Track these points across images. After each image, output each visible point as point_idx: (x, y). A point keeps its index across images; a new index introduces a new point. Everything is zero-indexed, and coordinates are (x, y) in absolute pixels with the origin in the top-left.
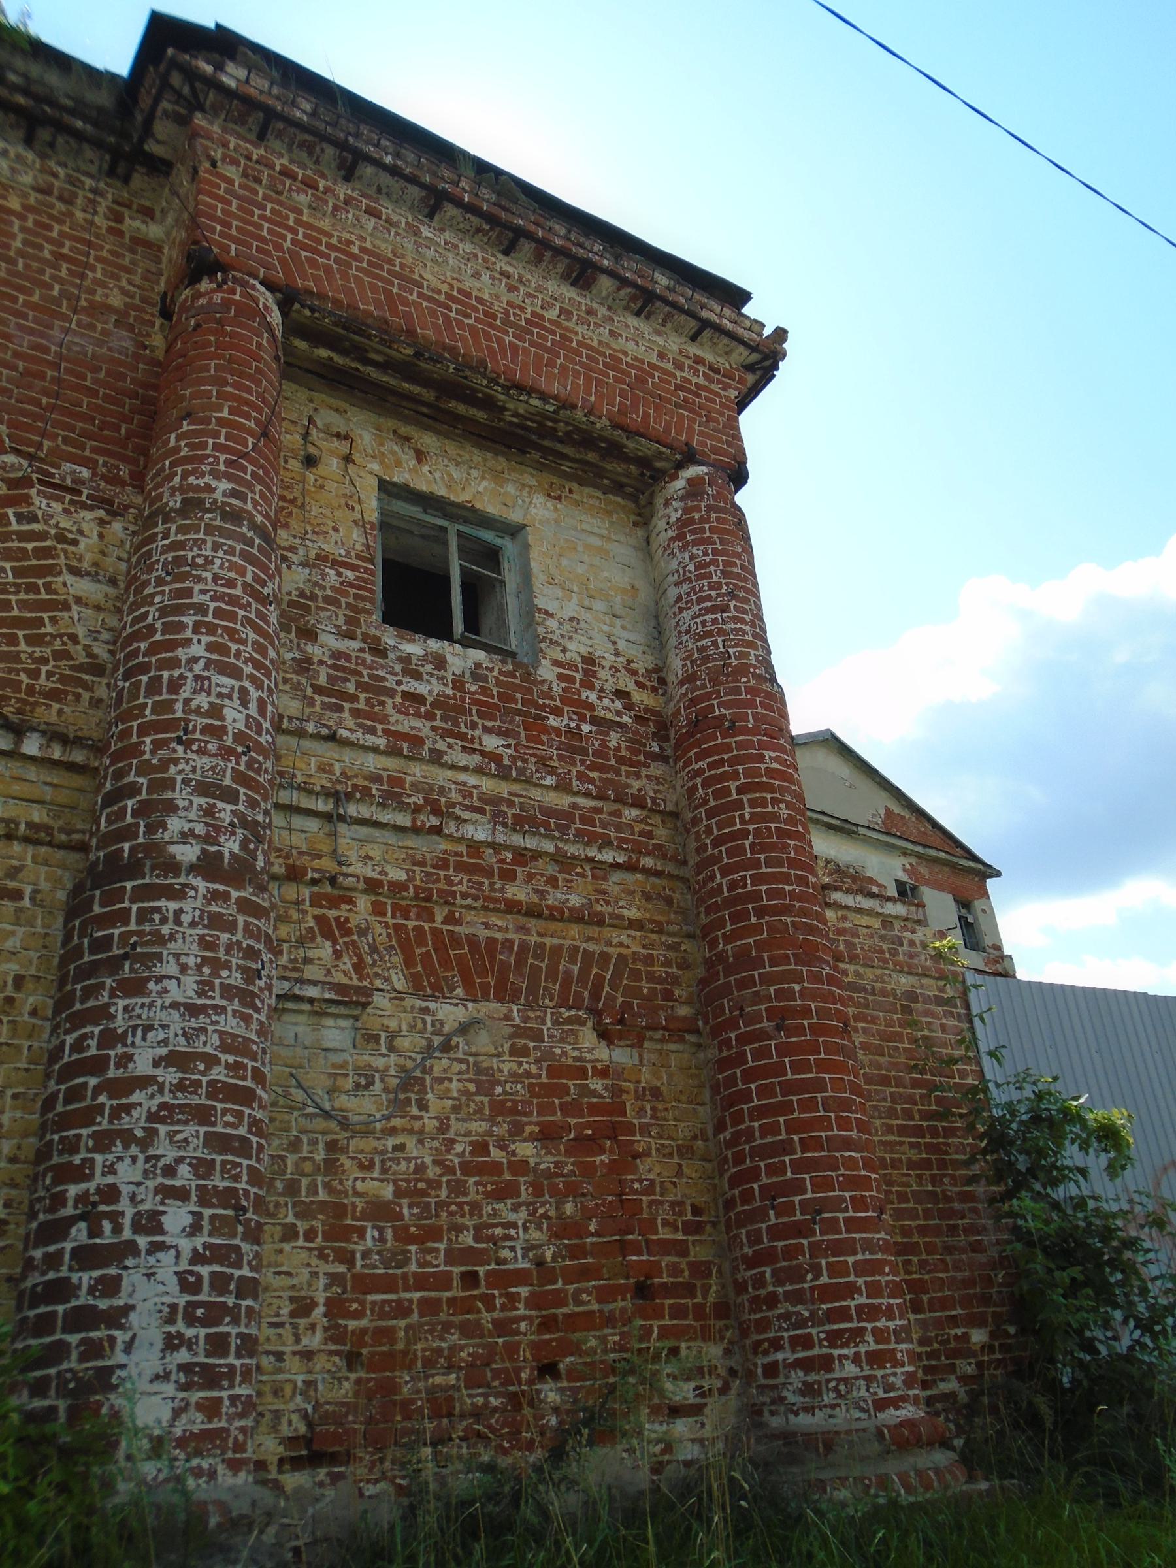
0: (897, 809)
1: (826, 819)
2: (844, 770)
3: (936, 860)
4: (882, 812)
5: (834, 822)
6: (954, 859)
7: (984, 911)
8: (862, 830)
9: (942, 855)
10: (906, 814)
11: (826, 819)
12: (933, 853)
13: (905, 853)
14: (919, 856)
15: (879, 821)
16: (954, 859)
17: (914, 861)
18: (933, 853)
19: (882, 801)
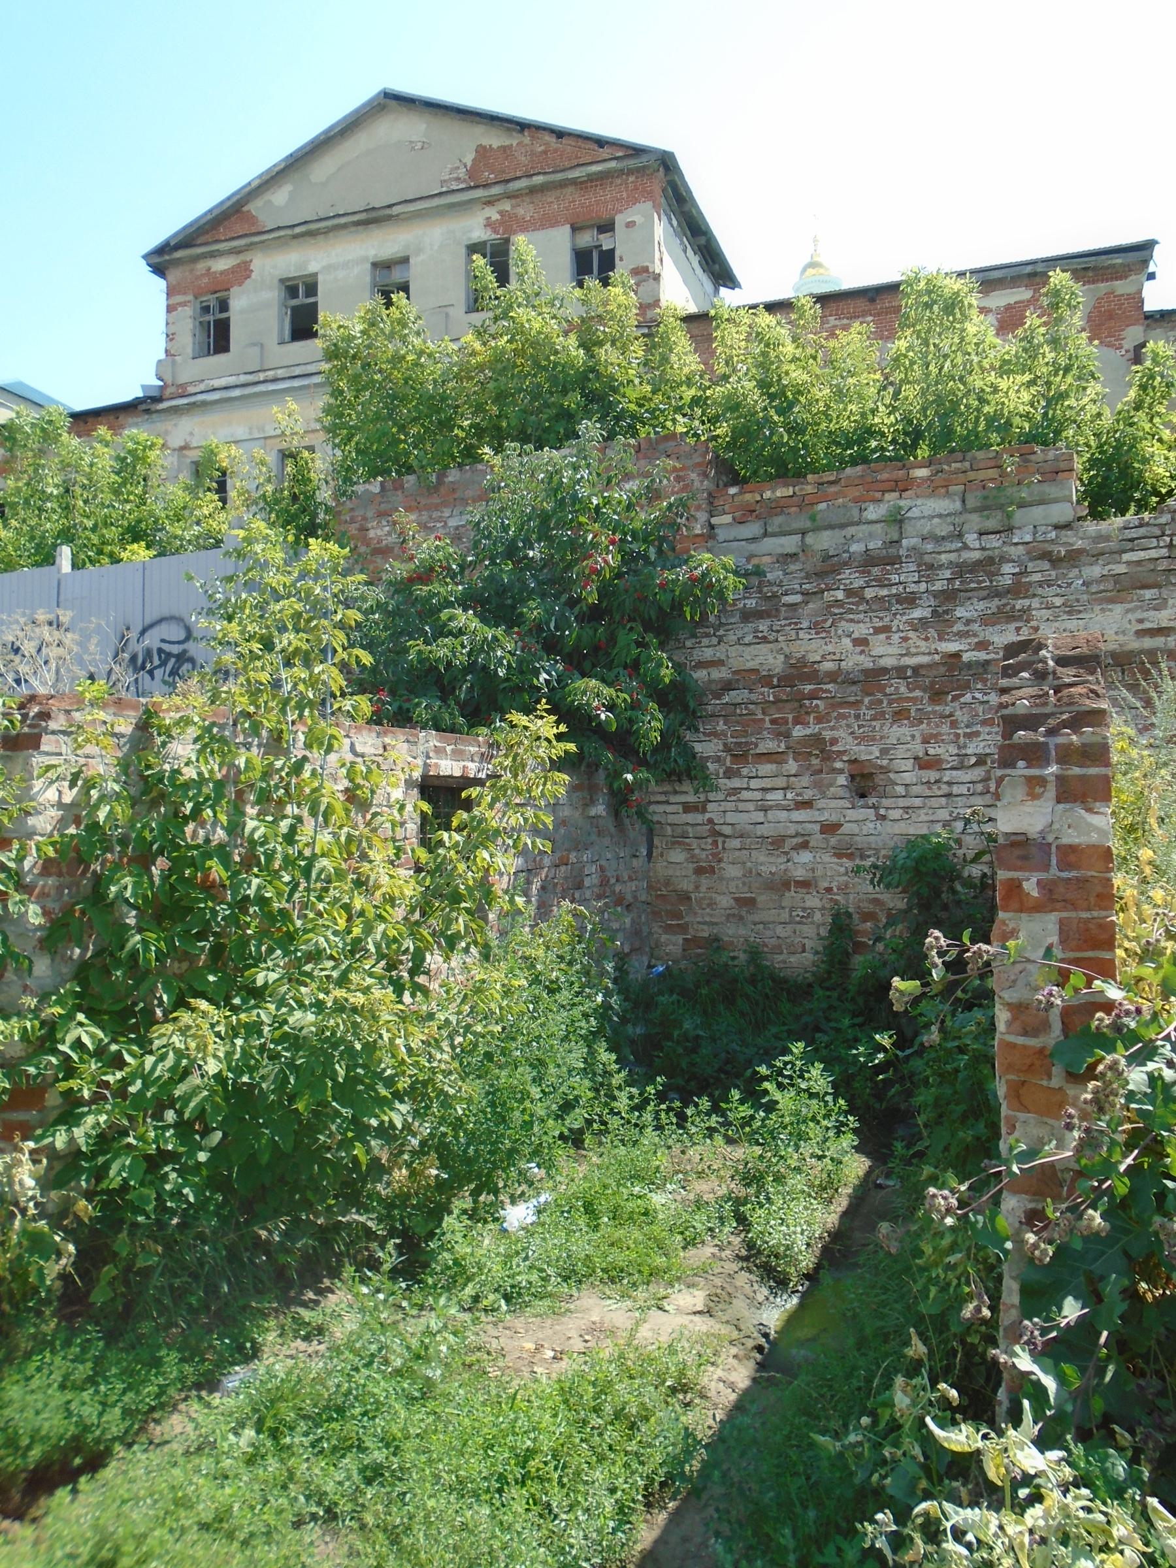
0: (495, 139)
1: (343, 220)
2: (412, 128)
3: (533, 191)
4: (469, 159)
5: (356, 218)
6: (559, 176)
7: (630, 225)
8: (396, 210)
9: (539, 180)
10: (513, 140)
11: (343, 220)
12: (523, 183)
13: (490, 202)
14: (509, 196)
15: (462, 173)
16: (559, 176)
17: (506, 206)
18: (523, 183)
19: (466, 144)
